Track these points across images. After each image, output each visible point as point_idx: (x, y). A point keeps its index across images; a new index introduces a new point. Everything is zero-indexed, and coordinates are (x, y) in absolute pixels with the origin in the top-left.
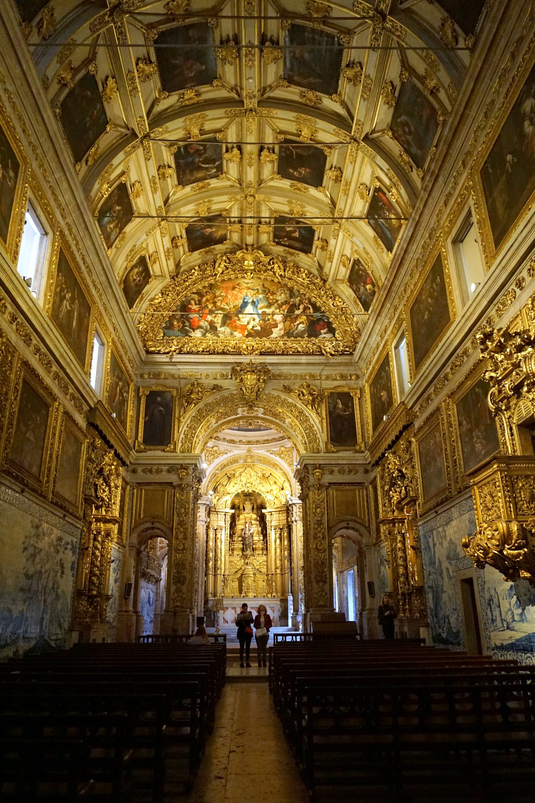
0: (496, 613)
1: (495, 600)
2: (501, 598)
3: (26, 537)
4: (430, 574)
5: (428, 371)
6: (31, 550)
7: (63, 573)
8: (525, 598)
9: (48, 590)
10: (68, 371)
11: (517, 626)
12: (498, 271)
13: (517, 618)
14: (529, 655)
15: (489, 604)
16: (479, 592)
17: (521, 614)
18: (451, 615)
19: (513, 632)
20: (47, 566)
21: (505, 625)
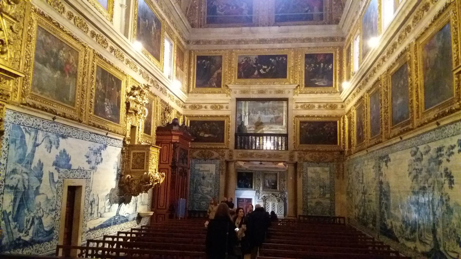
0: (95, 209)
1: (96, 202)
2: (100, 201)
3: (409, 165)
4: (14, 171)
5: (92, 13)
6: (414, 173)
7: (451, 182)
8: (113, 200)
9: (436, 203)
10: (406, 14)
11: (105, 215)
12: (145, 60)
13: (107, 210)
14: (109, 228)
15: (91, 204)
16: (85, 197)
17: (110, 208)
18: (45, 215)
19: (103, 218)
20: (430, 180)
21: (99, 216)
